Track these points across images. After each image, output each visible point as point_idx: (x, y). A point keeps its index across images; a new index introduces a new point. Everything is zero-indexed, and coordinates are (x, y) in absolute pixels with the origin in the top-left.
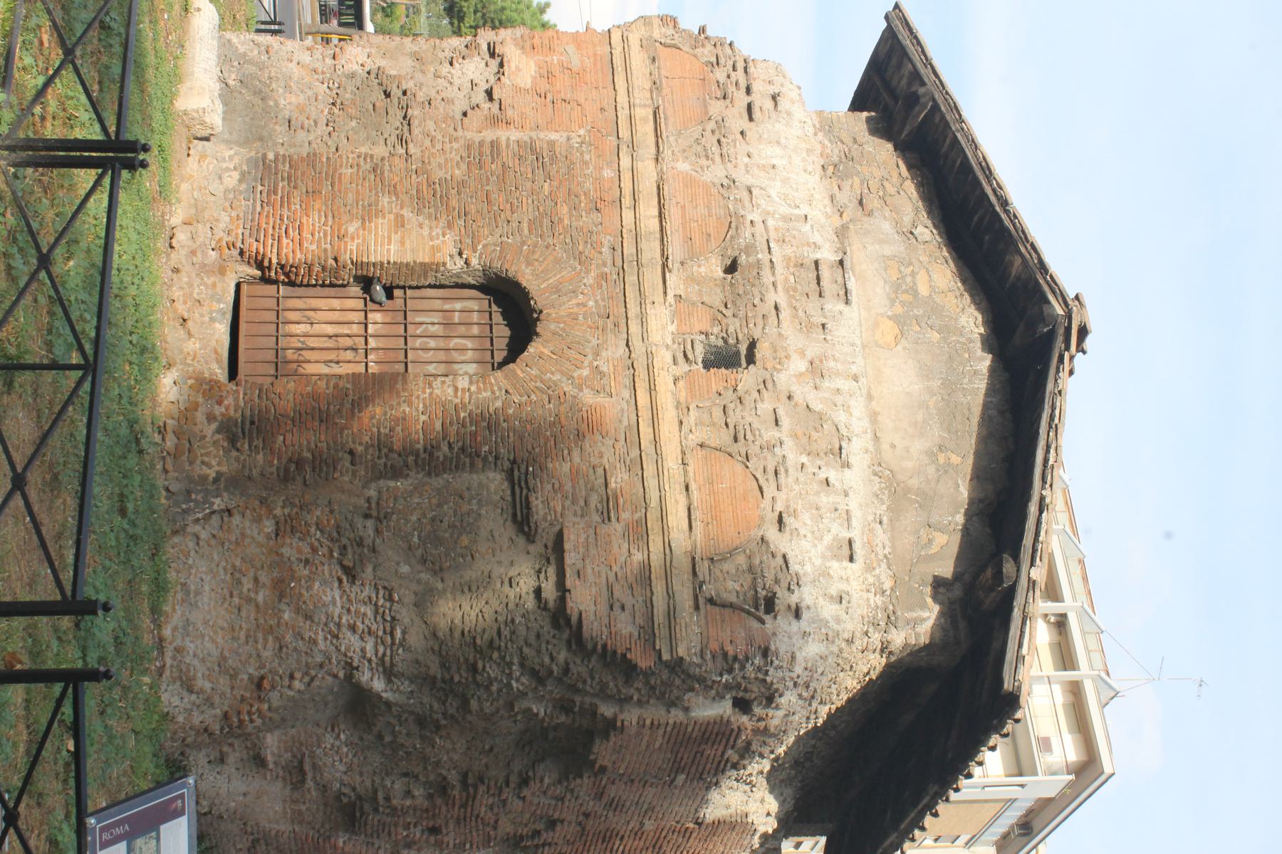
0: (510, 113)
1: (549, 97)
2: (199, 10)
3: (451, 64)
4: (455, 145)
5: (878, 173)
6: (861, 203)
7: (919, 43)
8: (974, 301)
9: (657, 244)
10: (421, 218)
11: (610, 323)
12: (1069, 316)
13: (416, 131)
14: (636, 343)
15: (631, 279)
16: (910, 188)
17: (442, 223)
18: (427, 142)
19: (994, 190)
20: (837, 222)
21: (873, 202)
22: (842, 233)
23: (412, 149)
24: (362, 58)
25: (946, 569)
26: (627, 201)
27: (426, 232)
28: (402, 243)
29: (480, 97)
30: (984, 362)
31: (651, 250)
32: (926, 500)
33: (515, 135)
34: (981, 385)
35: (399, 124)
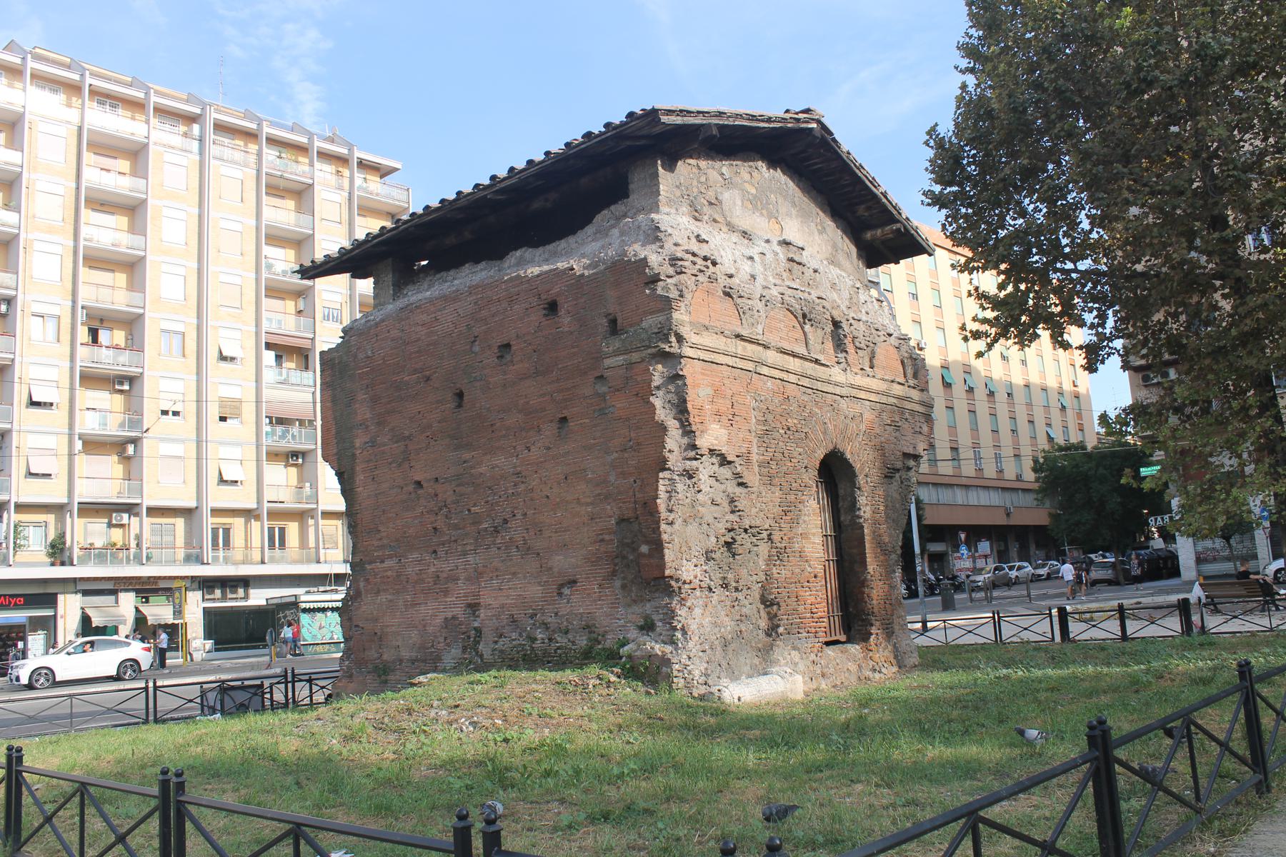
0: (744, 450)
1: (731, 417)
2: (739, 699)
3: (699, 491)
4: (764, 494)
5: (695, 183)
6: (711, 204)
7: (681, 111)
8: (753, 161)
9: (807, 364)
10: (801, 521)
11: (835, 405)
12: (819, 122)
13: (758, 523)
14: (844, 391)
15: (819, 386)
16: (703, 163)
17: (801, 506)
18: (761, 514)
19: (763, 121)
20: (725, 229)
21: (711, 195)
22: (732, 228)
23: (767, 526)
24: (690, 566)
25: (854, 250)
26: (784, 376)
27: (806, 518)
28: (814, 534)
29: (725, 472)
30: (778, 174)
31: (810, 368)
32: (835, 246)
33: (755, 450)
34: (791, 184)
35: (746, 536)
